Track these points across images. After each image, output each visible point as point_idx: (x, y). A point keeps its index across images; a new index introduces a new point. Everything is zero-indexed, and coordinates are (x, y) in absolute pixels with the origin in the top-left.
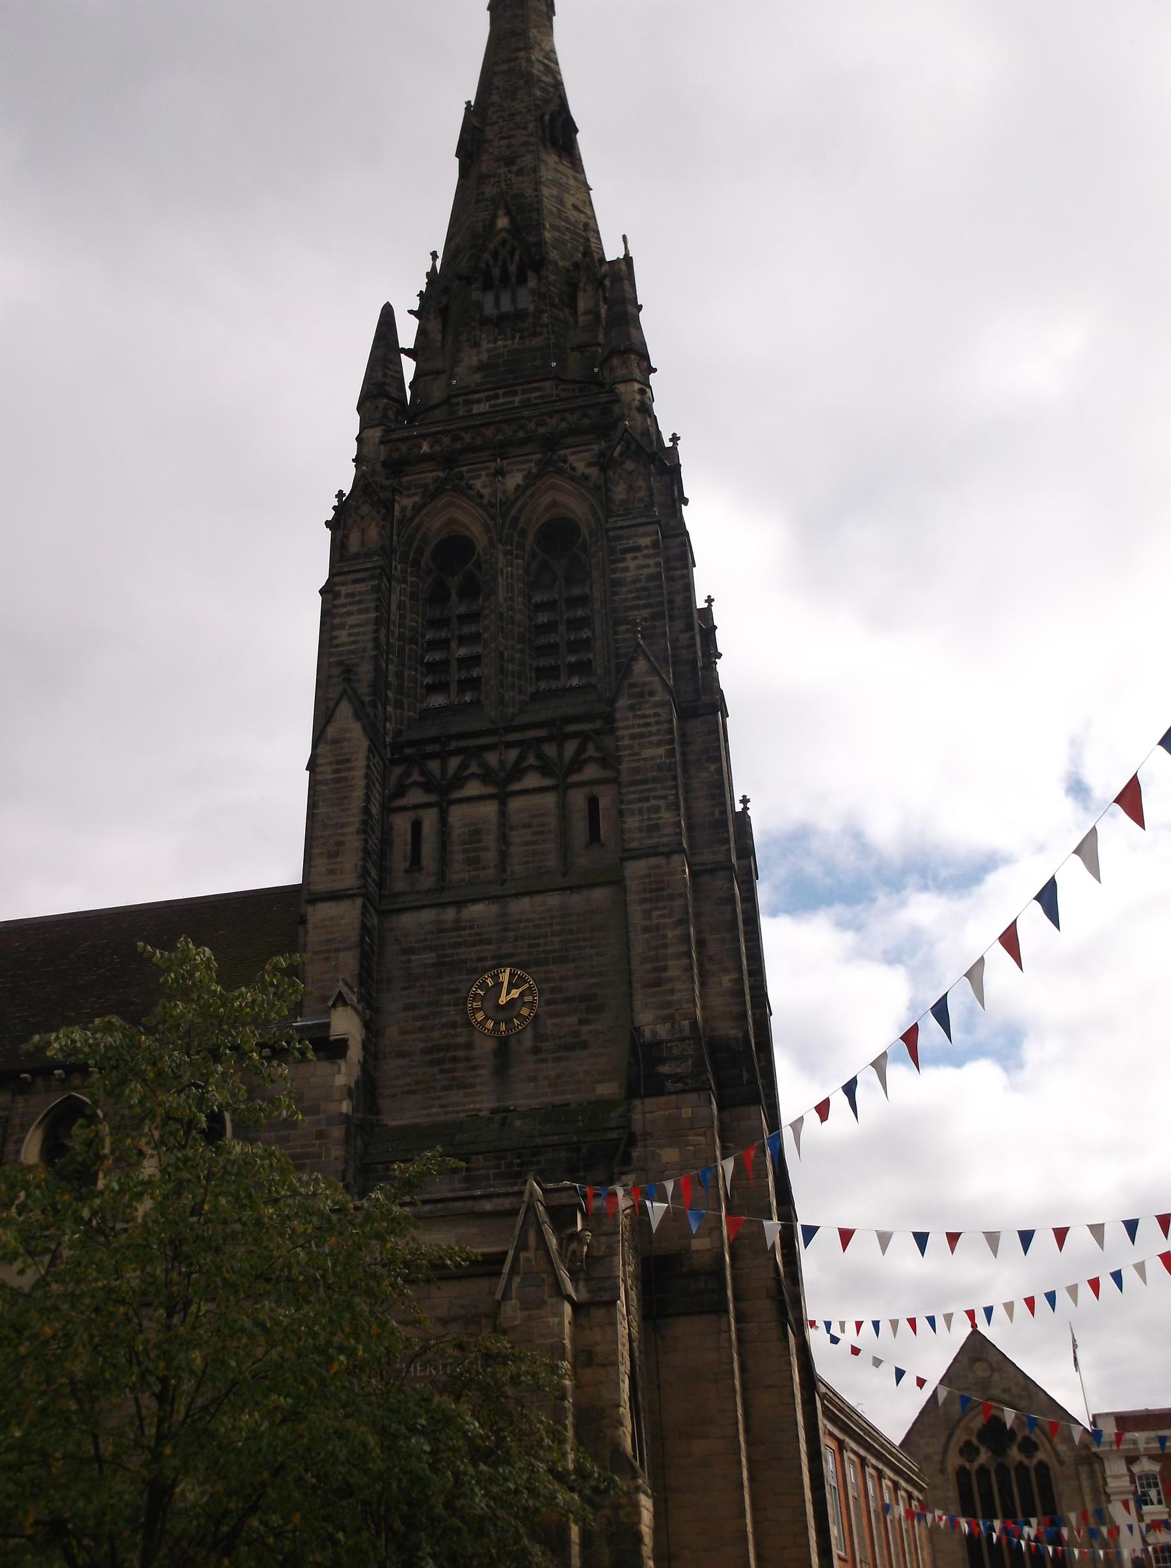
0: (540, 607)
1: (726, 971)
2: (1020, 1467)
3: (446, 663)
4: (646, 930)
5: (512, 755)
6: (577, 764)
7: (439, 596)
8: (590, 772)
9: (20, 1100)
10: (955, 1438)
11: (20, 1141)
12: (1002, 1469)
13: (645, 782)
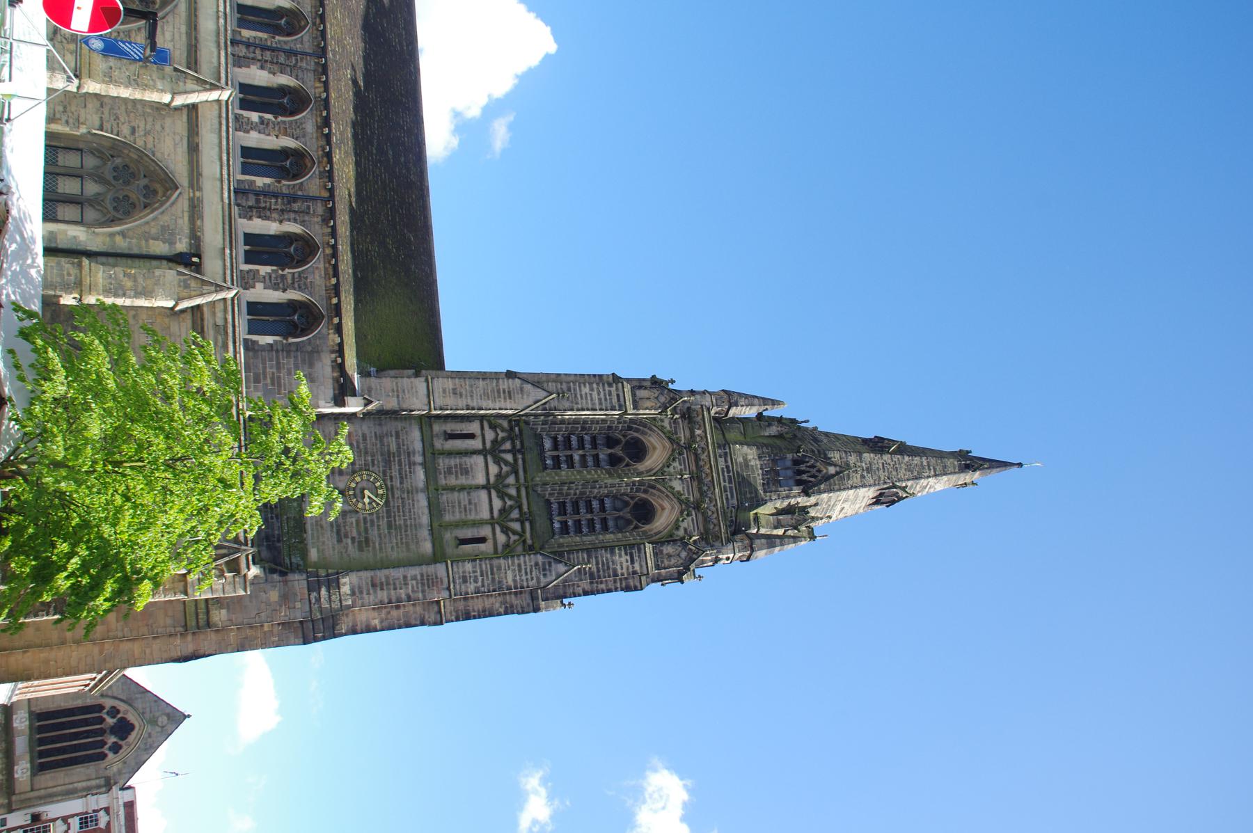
0: (602, 502)
1: (381, 622)
2: (104, 743)
4: (405, 577)
5: (513, 492)
6: (506, 530)
7: (611, 442)
8: (501, 538)
9: (319, 219)
10: (122, 704)
11: (295, 221)
12: (102, 732)
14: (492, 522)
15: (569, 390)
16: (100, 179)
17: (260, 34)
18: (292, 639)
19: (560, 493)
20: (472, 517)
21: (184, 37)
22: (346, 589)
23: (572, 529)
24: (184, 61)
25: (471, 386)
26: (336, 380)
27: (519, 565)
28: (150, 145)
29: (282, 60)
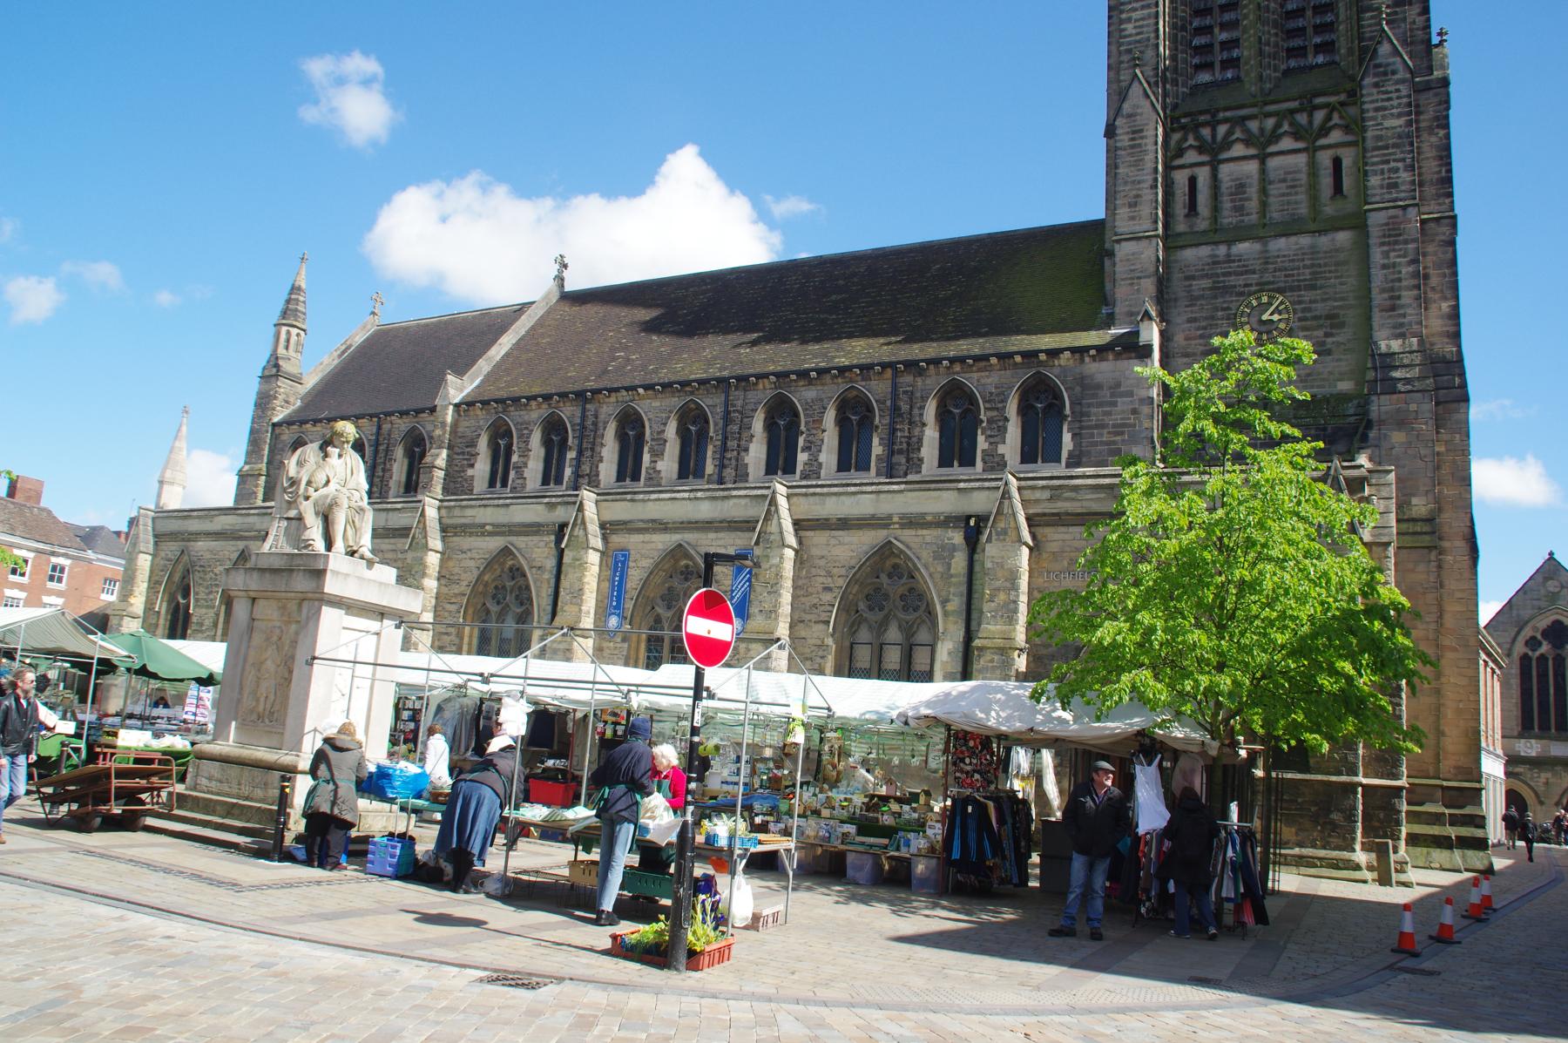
1: (1445, 299)
3: (1211, 45)
4: (1384, 267)
5: (1270, 122)
6: (1324, 131)
8: (1336, 136)
9: (919, 379)
10: (1523, 633)
11: (922, 408)
13: (1386, 147)
14: (1312, 150)
15: (1129, 51)
16: (883, 626)
17: (709, 453)
18: (1456, 416)
19: (1275, 56)
20: (1303, 177)
21: (721, 535)
22: (1396, 345)
23: (1327, 37)
24: (747, 535)
25: (1126, 183)
26: (1118, 356)
27: (1377, 110)
28: (843, 571)
29: (736, 428)
